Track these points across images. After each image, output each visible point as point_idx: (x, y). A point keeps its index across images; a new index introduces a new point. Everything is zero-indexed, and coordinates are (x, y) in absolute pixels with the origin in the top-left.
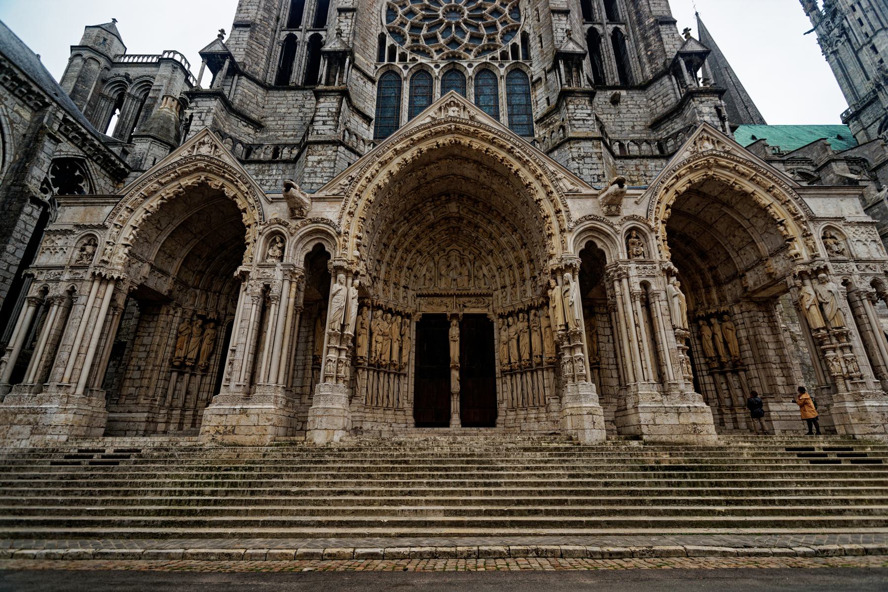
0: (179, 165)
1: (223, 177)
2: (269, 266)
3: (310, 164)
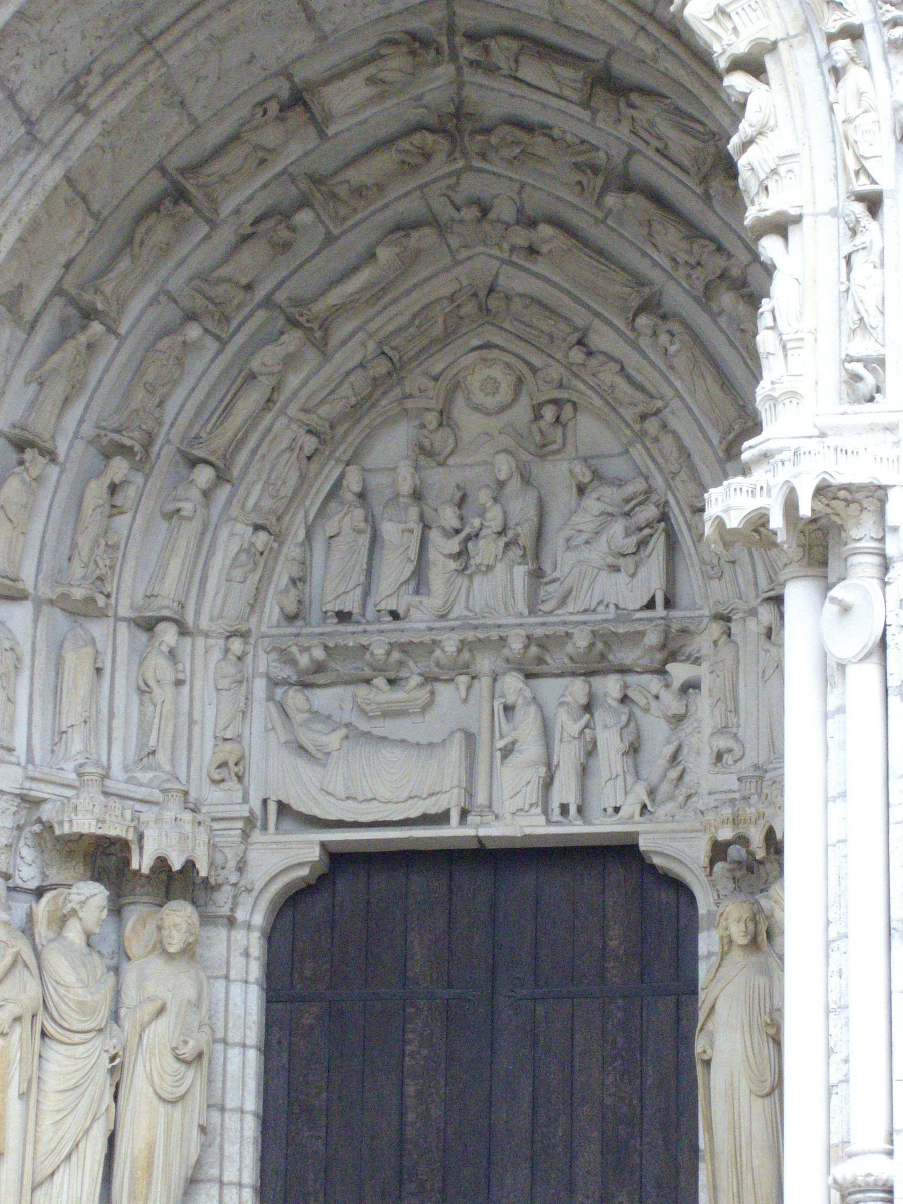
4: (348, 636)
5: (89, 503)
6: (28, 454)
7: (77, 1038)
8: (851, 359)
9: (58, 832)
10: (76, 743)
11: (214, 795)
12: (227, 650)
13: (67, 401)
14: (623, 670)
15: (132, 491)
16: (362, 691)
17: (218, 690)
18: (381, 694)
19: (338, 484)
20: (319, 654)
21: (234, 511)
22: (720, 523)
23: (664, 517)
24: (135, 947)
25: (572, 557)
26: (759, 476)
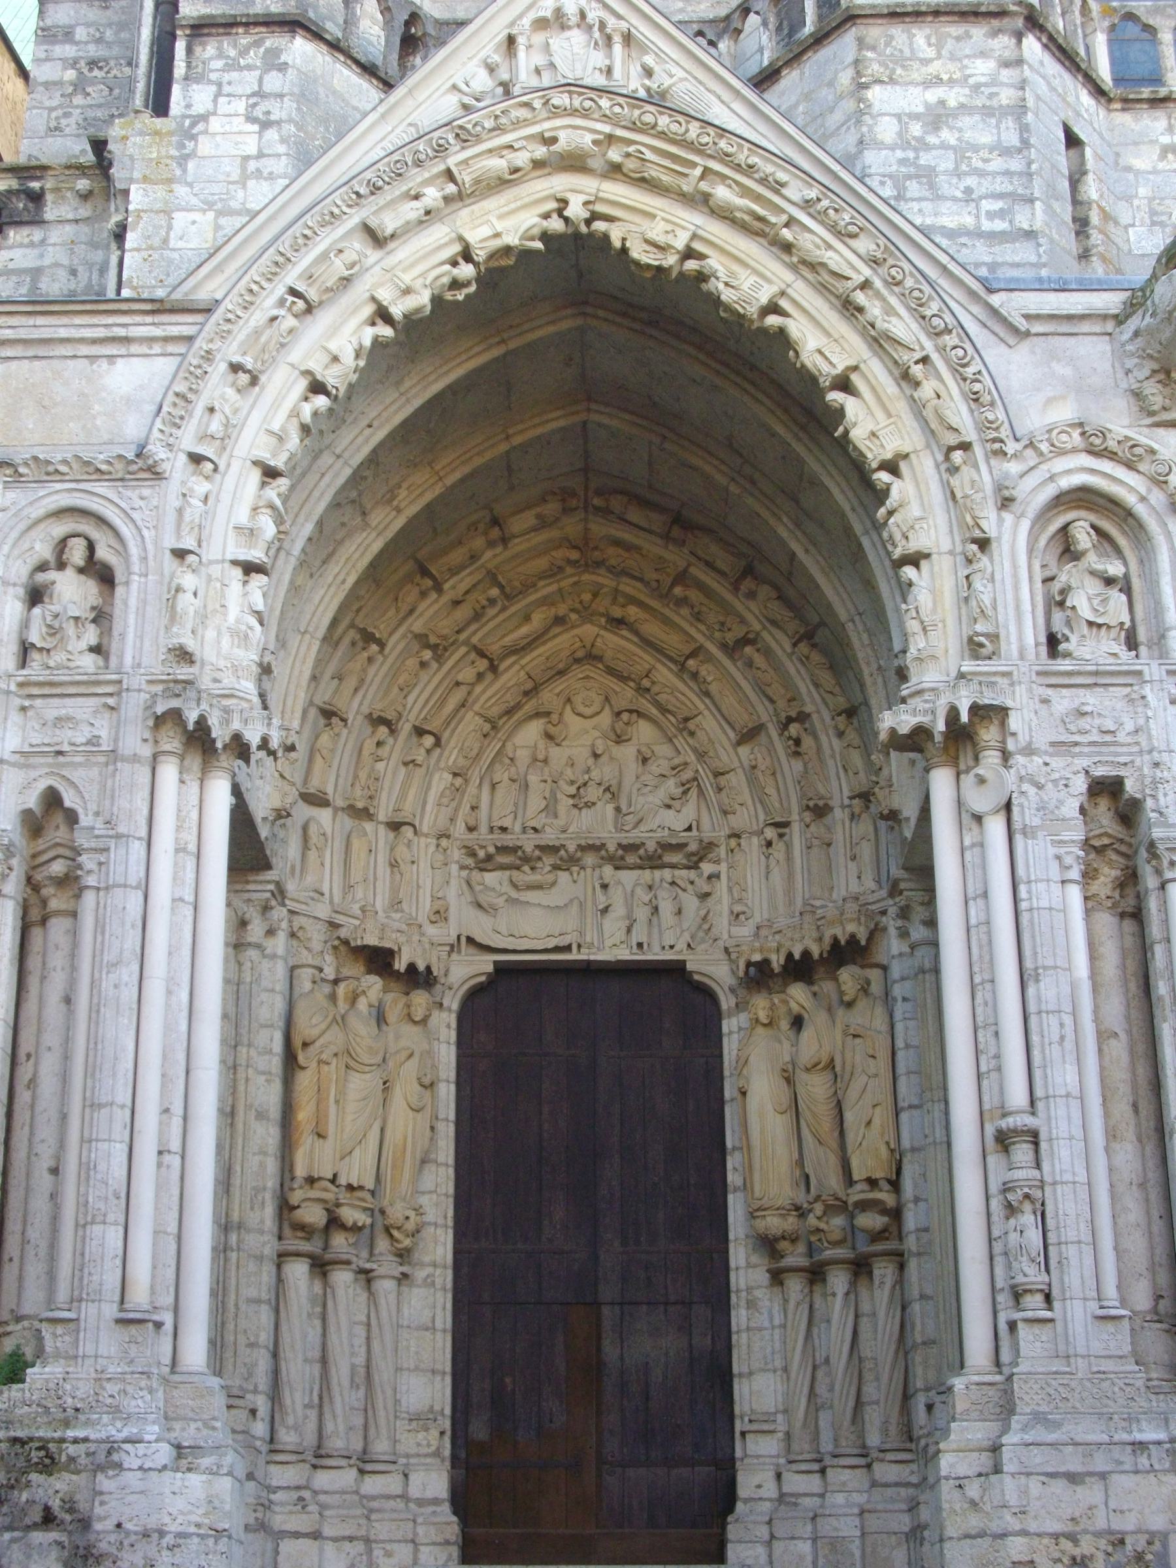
0: (464, 138)
1: (702, 201)
2: (1099, 679)
3: (887, 130)
4: (508, 840)
5: (365, 753)
6: (334, 720)
7: (367, 1069)
10: (360, 894)
11: (431, 931)
12: (438, 846)
13: (356, 690)
14: (673, 866)
15: (387, 748)
16: (515, 873)
18: (526, 876)
20: (491, 850)
21: (442, 765)
22: (893, 731)
23: (695, 779)
24: (392, 1016)
25: (641, 800)
26: (913, 702)
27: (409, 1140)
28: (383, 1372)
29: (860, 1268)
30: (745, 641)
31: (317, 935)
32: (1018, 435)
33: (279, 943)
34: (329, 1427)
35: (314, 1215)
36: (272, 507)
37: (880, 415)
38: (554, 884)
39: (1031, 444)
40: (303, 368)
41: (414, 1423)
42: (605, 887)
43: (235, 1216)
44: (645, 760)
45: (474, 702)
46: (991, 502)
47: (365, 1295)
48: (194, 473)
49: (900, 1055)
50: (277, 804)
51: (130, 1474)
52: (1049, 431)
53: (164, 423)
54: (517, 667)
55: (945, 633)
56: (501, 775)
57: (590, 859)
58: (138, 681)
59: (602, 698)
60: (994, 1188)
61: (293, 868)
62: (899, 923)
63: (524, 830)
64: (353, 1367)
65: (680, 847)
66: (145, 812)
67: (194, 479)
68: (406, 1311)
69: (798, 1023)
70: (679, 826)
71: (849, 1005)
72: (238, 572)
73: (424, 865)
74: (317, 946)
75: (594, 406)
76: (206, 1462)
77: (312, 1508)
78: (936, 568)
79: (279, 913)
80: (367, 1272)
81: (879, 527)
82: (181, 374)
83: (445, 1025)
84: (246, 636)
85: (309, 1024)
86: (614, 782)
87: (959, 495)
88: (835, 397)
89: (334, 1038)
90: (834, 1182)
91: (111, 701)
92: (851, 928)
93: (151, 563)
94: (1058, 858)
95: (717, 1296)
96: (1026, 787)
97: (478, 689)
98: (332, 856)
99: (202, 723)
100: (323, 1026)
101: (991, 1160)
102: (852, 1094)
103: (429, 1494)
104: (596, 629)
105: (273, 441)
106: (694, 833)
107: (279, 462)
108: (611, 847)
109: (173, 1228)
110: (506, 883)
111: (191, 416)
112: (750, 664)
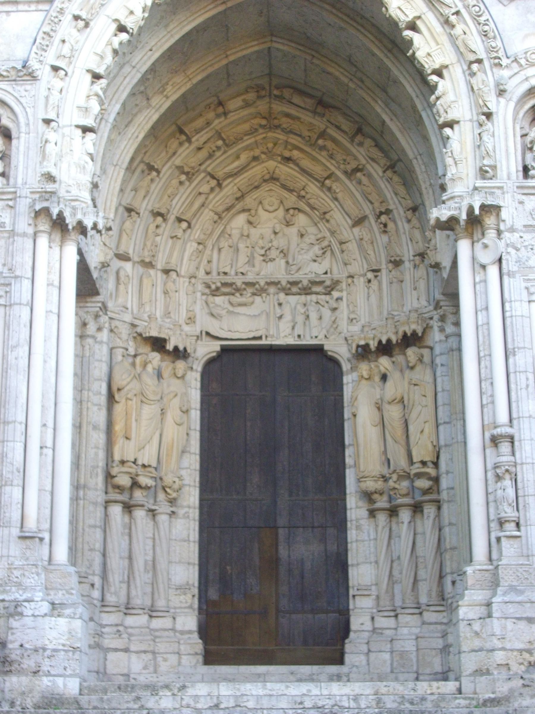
5: (150, 231)
6: (133, 213)
7: (152, 402)
8: (485, 166)
9: (144, 336)
10: (147, 309)
11: (186, 328)
12: (190, 282)
13: (145, 197)
14: (317, 293)
16: (232, 297)
17: (187, 294)
19: (223, 232)
20: (219, 284)
21: (192, 238)
22: (438, 219)
25: (300, 257)
26: (449, 203)
27: (175, 440)
28: (162, 565)
29: (417, 508)
30: (358, 170)
31: (124, 331)
32: (509, 55)
33: (104, 335)
34: (133, 593)
35: (124, 481)
36: (97, 95)
37: (433, 44)
38: (253, 303)
39: (516, 60)
40: (114, 18)
41: (178, 592)
42: (280, 304)
43: (82, 481)
44: (302, 236)
45: (209, 204)
46: (493, 92)
47: (152, 523)
48: (54, 77)
49: (439, 395)
50: (102, 259)
51: (27, 618)
52: (526, 53)
53: (37, 49)
54: (232, 184)
55: (467, 165)
56: (224, 244)
57: (272, 290)
58: (25, 192)
59: (279, 201)
60: (489, 466)
61: (111, 294)
62: (440, 324)
63: (236, 274)
64: (146, 561)
65: (321, 283)
66: (31, 263)
67: (55, 79)
68: (174, 531)
69: (384, 378)
70: (321, 271)
71: (412, 368)
72: (79, 132)
73: (182, 293)
74: (124, 336)
75: (274, 39)
76: (68, 611)
77: (125, 636)
78: (462, 129)
79: (104, 319)
80: (152, 511)
81: (431, 106)
82: (47, 22)
83: (194, 379)
84: (84, 167)
85: (121, 378)
86: (285, 248)
87: (475, 88)
88: (407, 33)
89: (135, 386)
90: (403, 463)
91: (11, 203)
92: (414, 327)
93: (32, 127)
94: (527, 288)
95: (341, 524)
96: (510, 250)
97: (211, 196)
98: (132, 288)
99: (60, 216)
100: (129, 380)
101: (488, 451)
102: (413, 415)
103: (187, 628)
104: (275, 164)
105: (98, 58)
106: (329, 275)
107: (101, 70)
108: (284, 283)
109: (49, 487)
110: (227, 302)
111: (52, 45)
112: (360, 182)
